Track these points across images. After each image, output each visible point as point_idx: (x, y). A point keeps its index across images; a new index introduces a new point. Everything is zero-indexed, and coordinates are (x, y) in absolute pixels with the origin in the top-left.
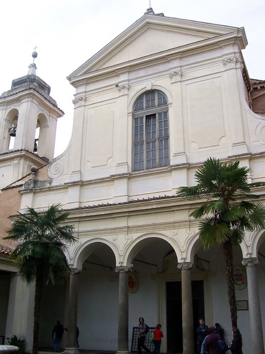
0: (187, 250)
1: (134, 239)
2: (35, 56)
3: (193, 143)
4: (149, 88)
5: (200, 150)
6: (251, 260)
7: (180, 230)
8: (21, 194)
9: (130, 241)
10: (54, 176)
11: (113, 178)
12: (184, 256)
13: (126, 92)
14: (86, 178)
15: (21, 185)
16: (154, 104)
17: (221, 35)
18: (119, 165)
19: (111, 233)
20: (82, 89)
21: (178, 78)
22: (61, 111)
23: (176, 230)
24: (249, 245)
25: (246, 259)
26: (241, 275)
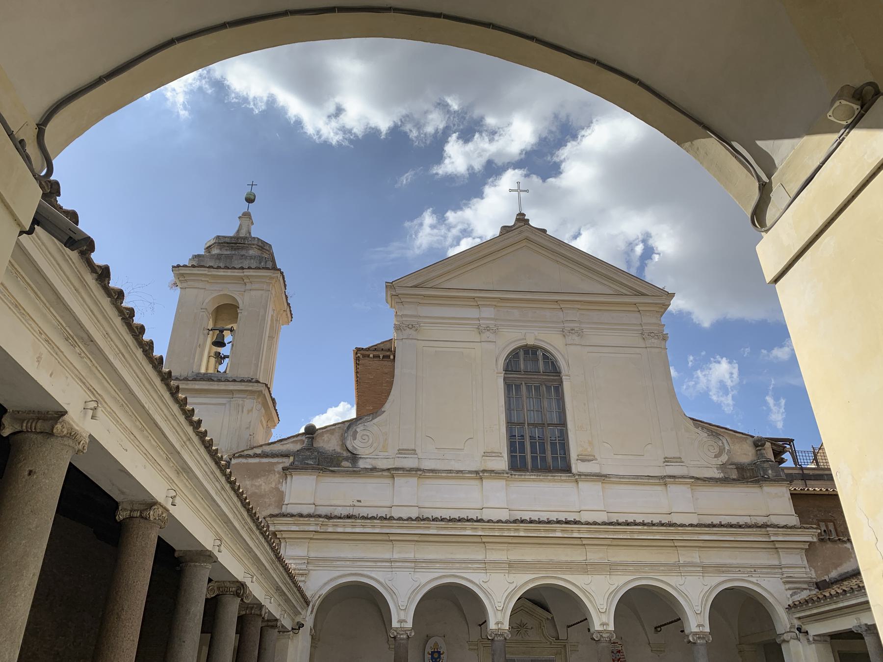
0: (609, 612)
1: (520, 583)
2: (250, 200)
3: (604, 443)
4: (531, 341)
5: (616, 457)
6: (700, 635)
7: (594, 576)
8: (287, 471)
9: (512, 587)
10: (360, 451)
11: (480, 475)
12: (604, 619)
13: (492, 337)
14: (427, 465)
15: (286, 455)
16: (539, 368)
17: (643, 294)
18: (486, 454)
19: (478, 568)
20: (408, 310)
21: (576, 339)
22: (291, 314)
23: (590, 576)
24: (699, 612)
25: (695, 634)
26: (619, 652)
